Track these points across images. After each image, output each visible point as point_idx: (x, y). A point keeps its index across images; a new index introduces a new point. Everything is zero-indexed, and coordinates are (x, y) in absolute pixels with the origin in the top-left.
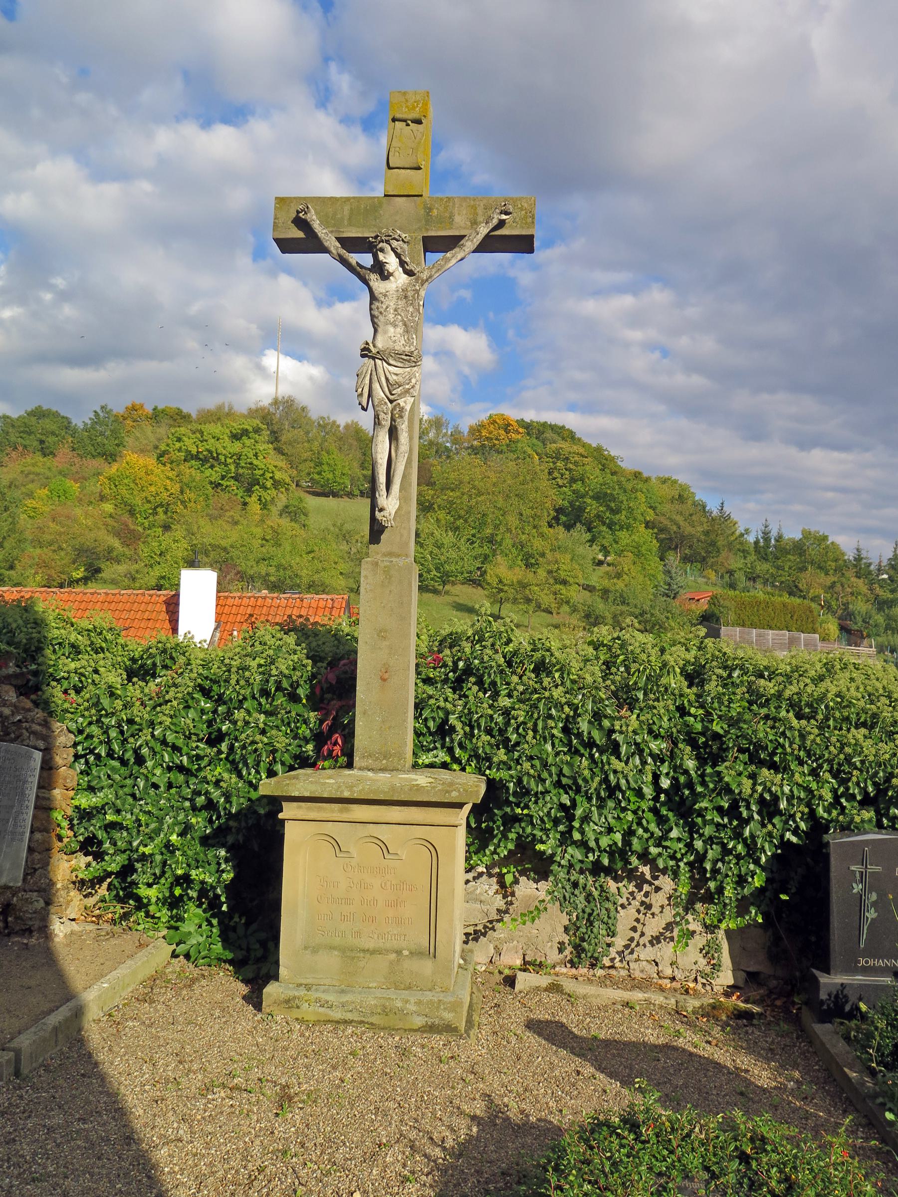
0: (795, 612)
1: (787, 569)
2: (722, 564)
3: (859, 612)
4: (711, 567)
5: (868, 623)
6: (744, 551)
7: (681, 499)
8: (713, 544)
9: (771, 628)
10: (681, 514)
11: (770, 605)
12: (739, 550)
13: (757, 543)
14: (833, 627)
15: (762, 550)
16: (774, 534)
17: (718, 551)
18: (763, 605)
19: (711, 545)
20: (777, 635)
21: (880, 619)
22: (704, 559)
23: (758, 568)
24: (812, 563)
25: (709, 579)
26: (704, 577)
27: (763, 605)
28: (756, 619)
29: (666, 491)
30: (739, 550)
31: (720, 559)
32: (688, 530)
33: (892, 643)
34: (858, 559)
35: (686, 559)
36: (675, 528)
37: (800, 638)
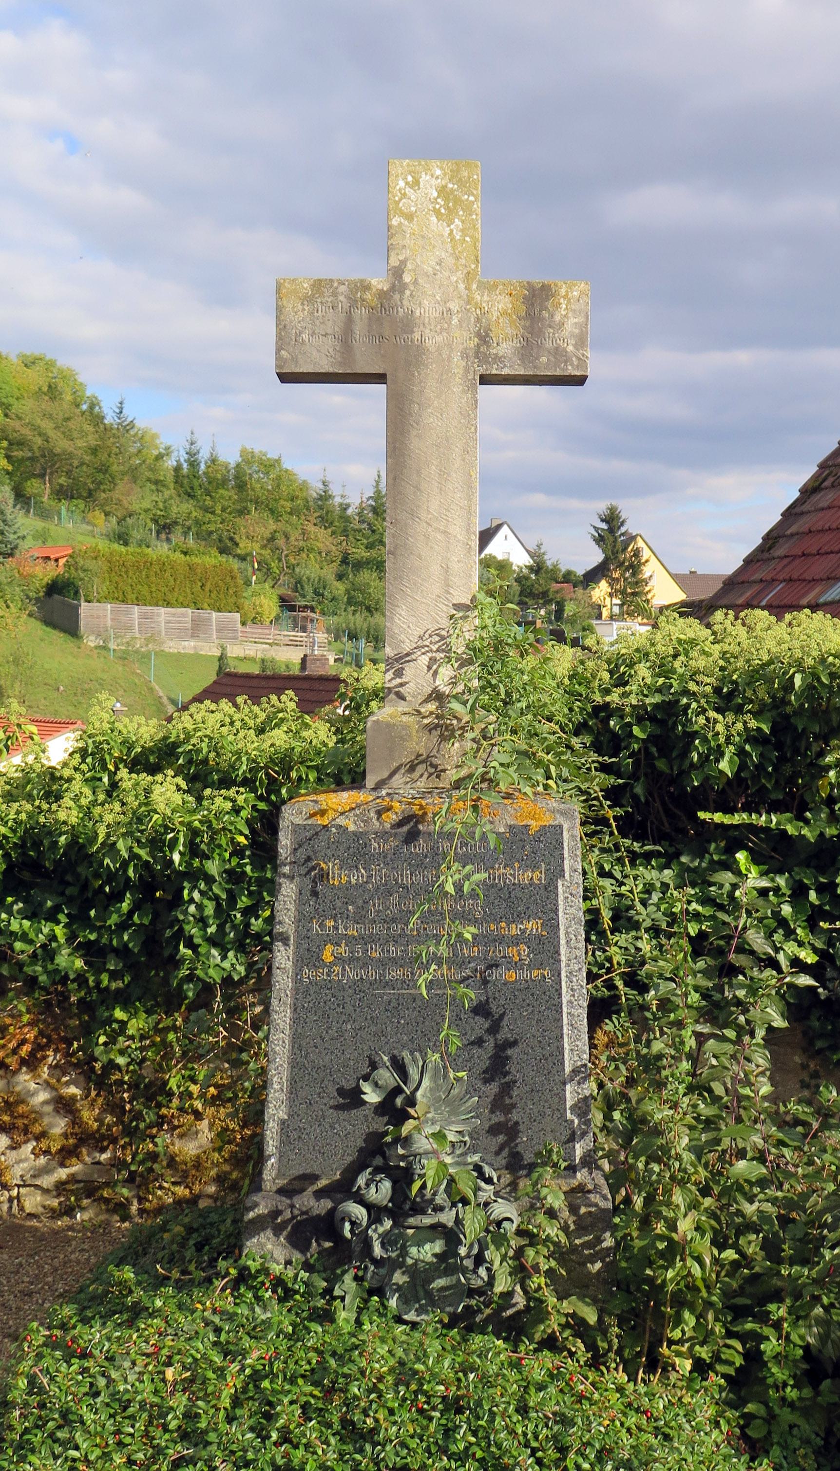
0: (207, 579)
1: (218, 512)
2: (119, 502)
3: (309, 579)
4: (102, 506)
5: (322, 595)
6: (157, 482)
7: (52, 392)
8: (104, 469)
9: (168, 604)
10: (51, 417)
11: (167, 567)
12: (149, 480)
13: (178, 469)
14: (269, 605)
15: (186, 481)
16: (204, 456)
17: (113, 481)
18: (156, 568)
19: (99, 471)
20: (174, 615)
21: (340, 588)
22: (90, 494)
23: (175, 509)
24: (257, 502)
25: (94, 525)
26: (88, 523)
27: (156, 568)
28: (145, 591)
29: (35, 378)
30: (149, 480)
31: (116, 495)
32: (61, 444)
33: (352, 626)
34: (325, 497)
35: (61, 494)
36: (39, 441)
37: (210, 619)
